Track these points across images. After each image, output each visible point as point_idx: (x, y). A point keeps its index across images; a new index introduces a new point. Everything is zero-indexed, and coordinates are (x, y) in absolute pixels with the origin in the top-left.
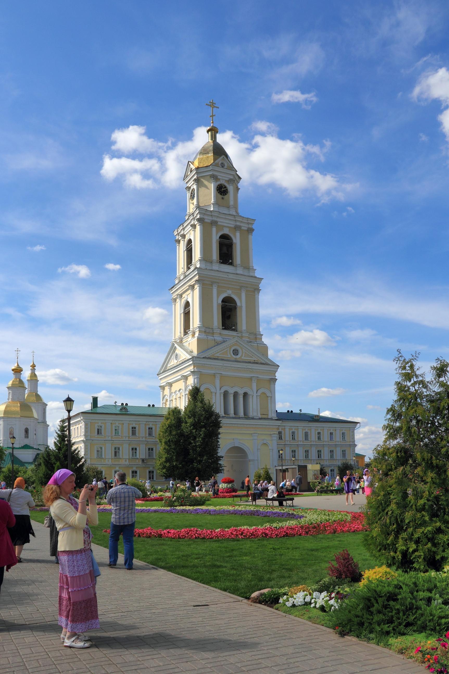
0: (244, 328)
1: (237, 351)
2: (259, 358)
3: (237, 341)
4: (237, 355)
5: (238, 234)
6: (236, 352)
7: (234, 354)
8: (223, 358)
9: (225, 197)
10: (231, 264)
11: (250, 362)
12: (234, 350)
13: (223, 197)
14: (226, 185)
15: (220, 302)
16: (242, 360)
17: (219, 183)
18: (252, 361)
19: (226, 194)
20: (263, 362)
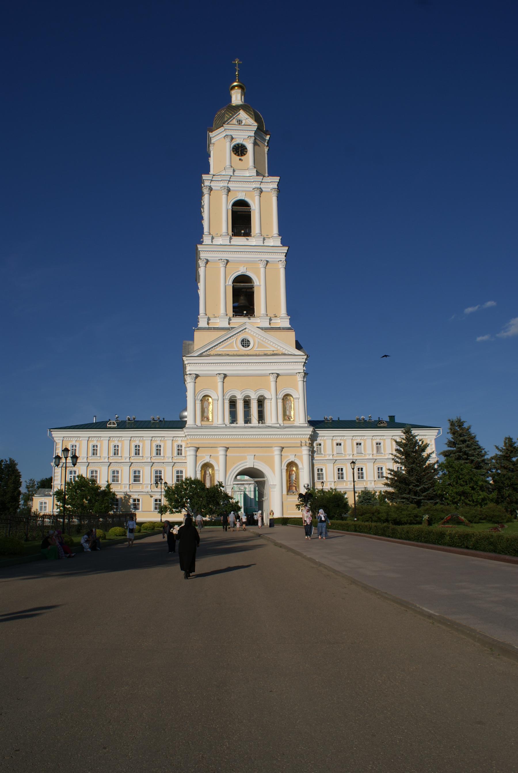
0: (263, 311)
1: (248, 341)
2: (279, 348)
3: (245, 329)
4: (248, 346)
5: (257, 198)
6: (245, 343)
7: (243, 346)
8: (227, 353)
9: (242, 158)
10: (248, 234)
11: (266, 355)
12: (243, 341)
13: (240, 157)
14: (245, 143)
15: (230, 282)
16: (254, 353)
17: (234, 143)
18: (269, 353)
19: (245, 154)
20: (286, 352)
